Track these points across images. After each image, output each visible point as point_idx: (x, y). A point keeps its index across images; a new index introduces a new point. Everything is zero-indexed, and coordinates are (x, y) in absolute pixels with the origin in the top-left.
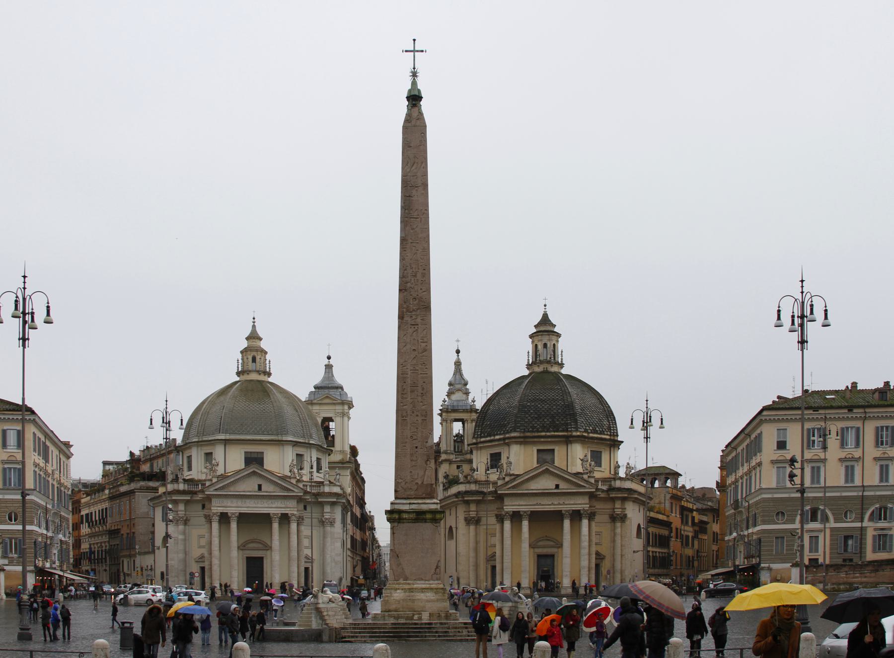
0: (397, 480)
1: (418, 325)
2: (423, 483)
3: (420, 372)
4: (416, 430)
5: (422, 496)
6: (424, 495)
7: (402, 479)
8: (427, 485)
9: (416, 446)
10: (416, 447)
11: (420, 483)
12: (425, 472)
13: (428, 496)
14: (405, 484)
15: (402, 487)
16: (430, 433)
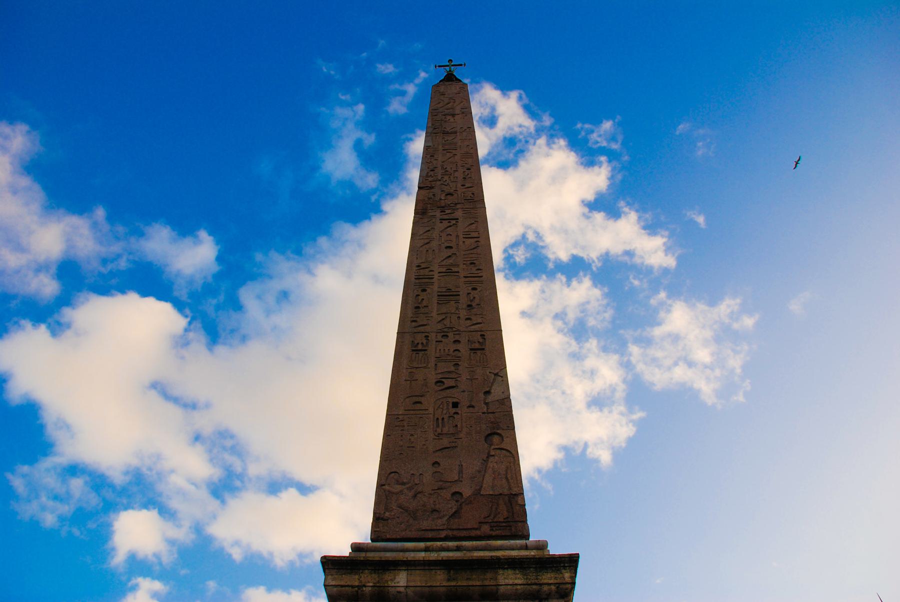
0: (387, 487)
1: (458, 219)
2: (480, 490)
3: (462, 274)
4: (453, 369)
5: (474, 533)
6: (486, 529)
7: (403, 484)
8: (495, 498)
9: (455, 400)
10: (455, 405)
11: (467, 492)
12: (486, 461)
13: (498, 532)
14: (415, 496)
15: (400, 507)
16: (496, 375)
